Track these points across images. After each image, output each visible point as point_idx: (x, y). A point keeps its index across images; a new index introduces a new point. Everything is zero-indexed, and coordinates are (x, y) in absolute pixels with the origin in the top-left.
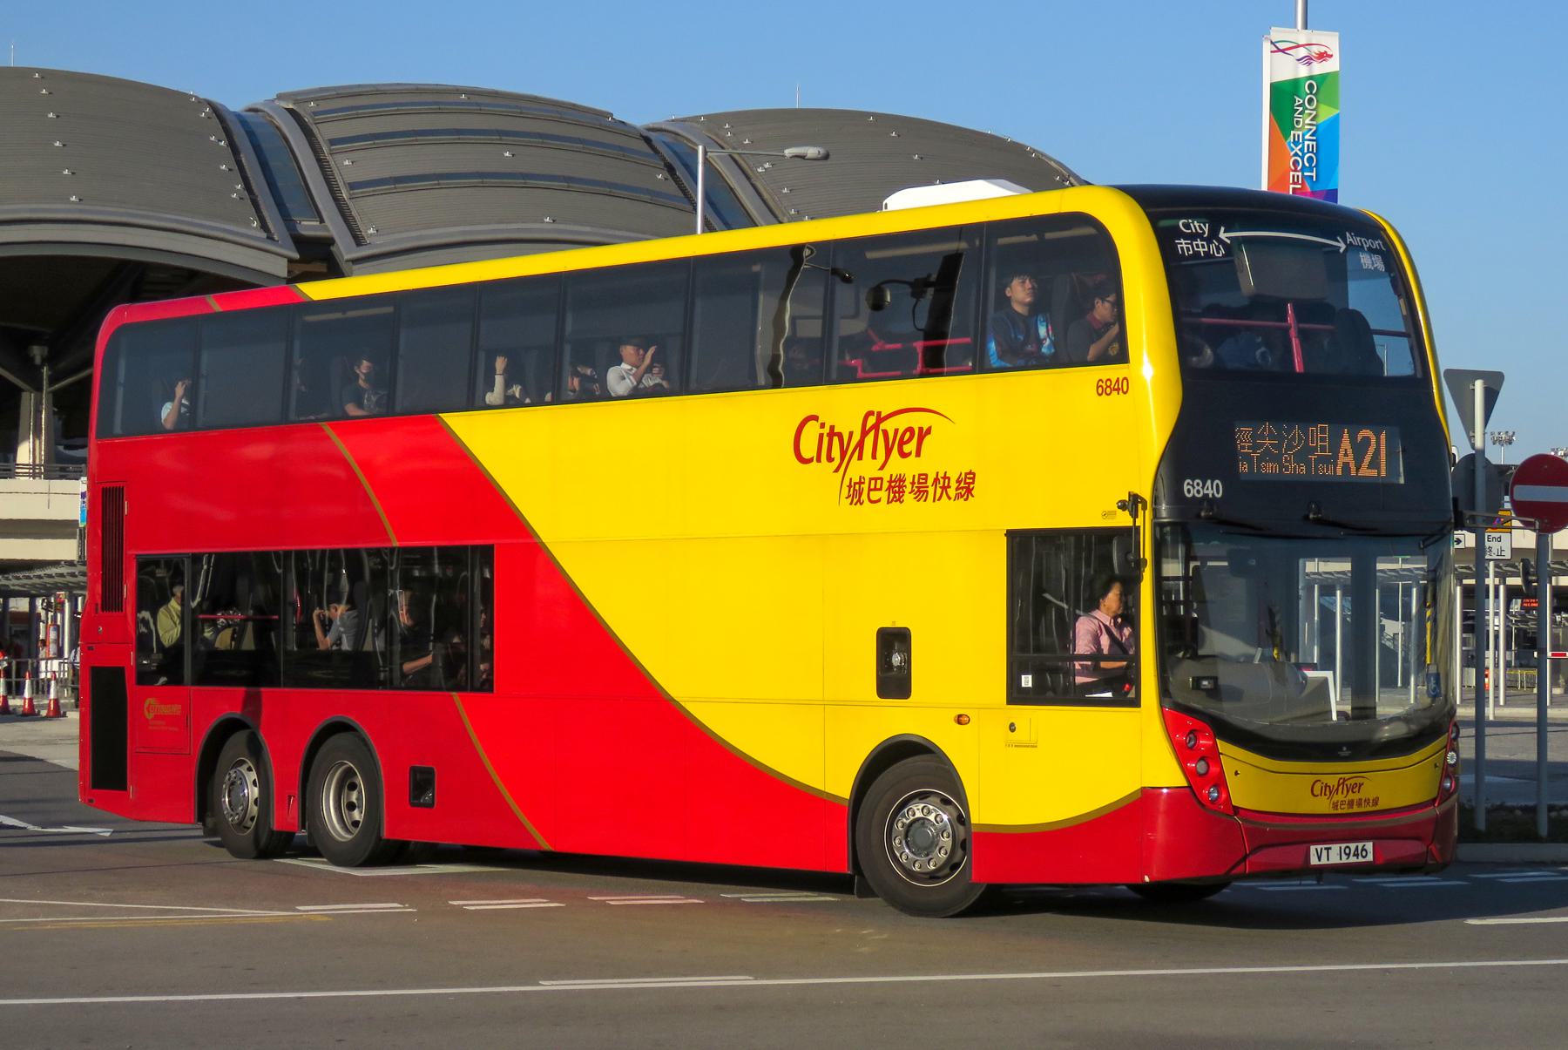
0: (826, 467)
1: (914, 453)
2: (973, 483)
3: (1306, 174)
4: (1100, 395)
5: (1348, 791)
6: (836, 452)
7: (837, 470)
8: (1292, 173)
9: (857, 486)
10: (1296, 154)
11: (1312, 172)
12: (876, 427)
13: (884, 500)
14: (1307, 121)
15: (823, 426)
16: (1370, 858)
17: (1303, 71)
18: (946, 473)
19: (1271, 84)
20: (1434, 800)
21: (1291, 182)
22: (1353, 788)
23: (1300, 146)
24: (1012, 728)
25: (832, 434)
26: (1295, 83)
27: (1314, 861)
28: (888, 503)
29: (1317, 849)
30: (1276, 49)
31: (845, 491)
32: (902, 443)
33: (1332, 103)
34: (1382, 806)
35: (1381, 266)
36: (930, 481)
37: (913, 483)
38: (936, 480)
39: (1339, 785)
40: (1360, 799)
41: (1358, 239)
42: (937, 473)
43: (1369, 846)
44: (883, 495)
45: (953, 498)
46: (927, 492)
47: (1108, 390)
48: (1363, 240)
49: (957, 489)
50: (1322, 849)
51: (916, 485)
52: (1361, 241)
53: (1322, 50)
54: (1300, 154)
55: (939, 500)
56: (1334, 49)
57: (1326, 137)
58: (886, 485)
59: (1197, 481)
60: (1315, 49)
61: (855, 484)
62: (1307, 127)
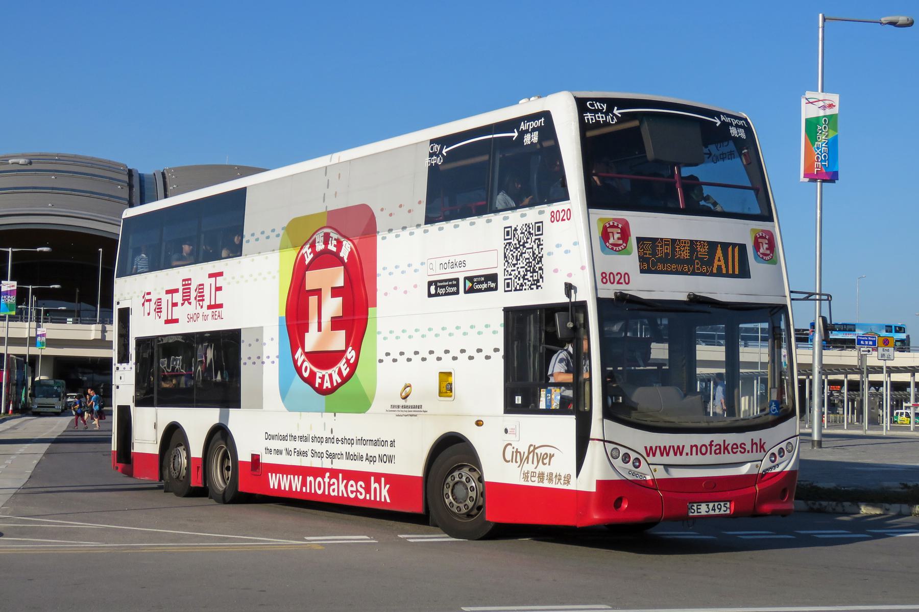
3: (823, 163)
8: (816, 163)
10: (818, 154)
11: (826, 162)
14: (823, 138)
17: (821, 113)
19: (806, 119)
21: (815, 167)
23: (820, 150)
26: (818, 118)
30: (808, 102)
33: (835, 130)
53: (831, 103)
54: (820, 153)
56: (837, 103)
57: (833, 145)
60: (827, 102)
62: (823, 140)
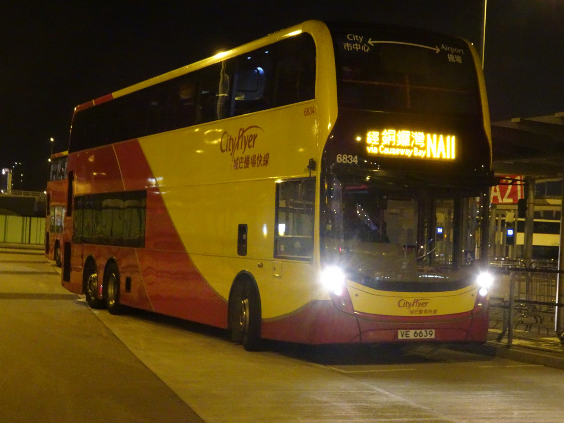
0: (229, 153)
1: (252, 146)
2: (268, 158)
4: (305, 115)
5: (419, 305)
6: (231, 148)
7: (231, 155)
9: (236, 162)
12: (242, 135)
13: (243, 167)
15: (228, 135)
16: (433, 337)
18: (261, 154)
20: (472, 311)
22: (422, 305)
24: (275, 268)
25: (231, 139)
27: (400, 337)
28: (245, 168)
29: (401, 332)
31: (233, 163)
32: (250, 141)
34: (438, 313)
35: (459, 60)
36: (257, 157)
37: (251, 159)
38: (258, 158)
39: (414, 302)
40: (426, 310)
41: (449, 48)
42: (258, 155)
43: (433, 331)
44: (243, 165)
45: (262, 164)
46: (255, 163)
47: (308, 113)
48: (451, 48)
49: (264, 161)
50: (404, 332)
51: (252, 160)
52: (450, 49)
55: (259, 166)
58: (244, 160)
59: (344, 155)
61: (236, 160)
